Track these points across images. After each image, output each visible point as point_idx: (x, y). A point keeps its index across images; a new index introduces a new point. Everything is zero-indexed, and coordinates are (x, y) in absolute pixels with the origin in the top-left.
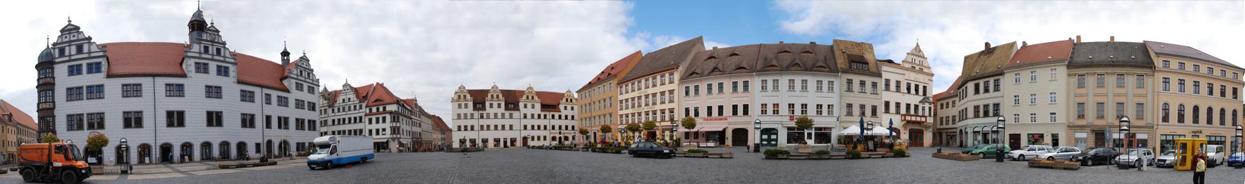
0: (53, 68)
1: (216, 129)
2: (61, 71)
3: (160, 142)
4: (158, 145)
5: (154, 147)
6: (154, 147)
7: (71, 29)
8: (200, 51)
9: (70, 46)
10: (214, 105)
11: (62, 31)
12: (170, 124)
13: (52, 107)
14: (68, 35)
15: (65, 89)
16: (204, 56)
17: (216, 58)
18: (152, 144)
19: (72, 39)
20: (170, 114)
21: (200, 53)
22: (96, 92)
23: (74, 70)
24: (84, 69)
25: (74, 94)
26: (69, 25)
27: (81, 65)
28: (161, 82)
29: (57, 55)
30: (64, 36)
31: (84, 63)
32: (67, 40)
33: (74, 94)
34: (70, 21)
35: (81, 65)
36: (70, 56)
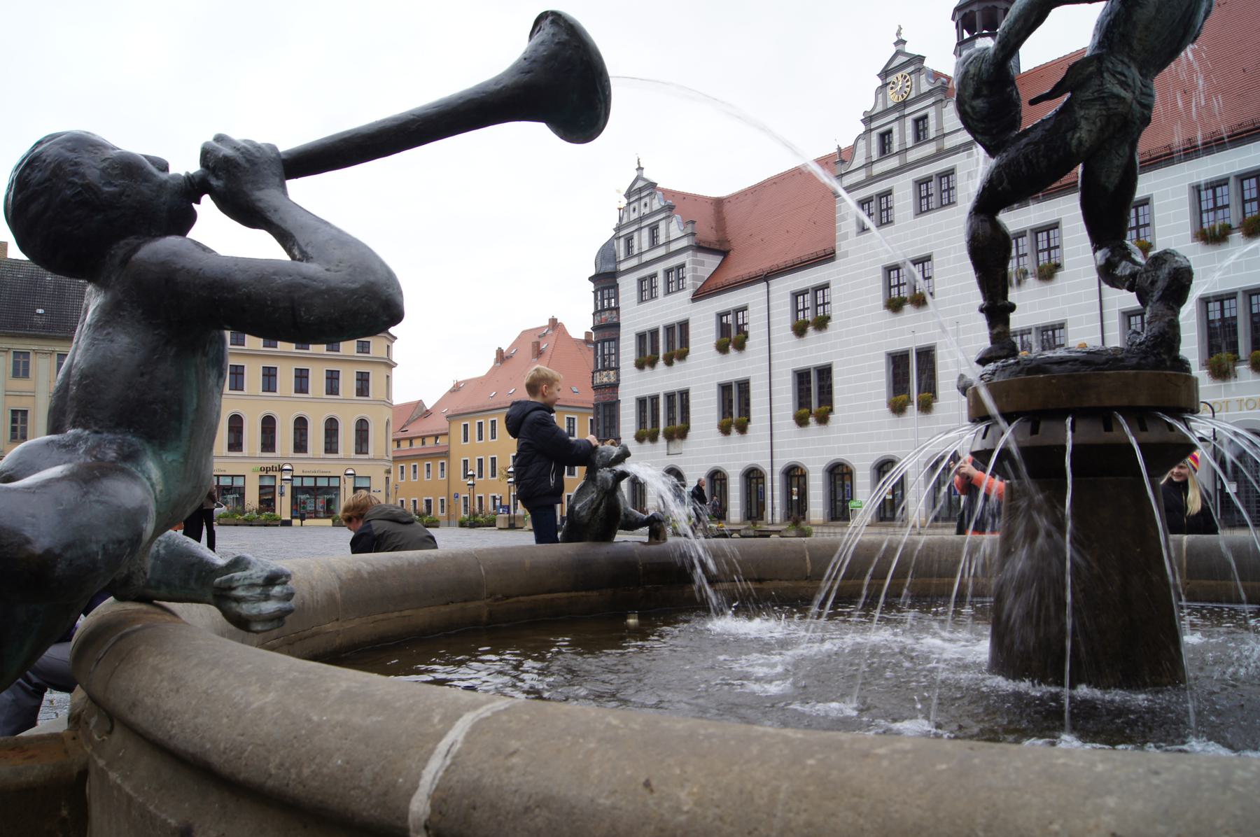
2: (628, 286)
4: (779, 468)
5: (769, 477)
6: (769, 477)
7: (640, 190)
9: (641, 228)
13: (613, 379)
15: (634, 335)
18: (766, 469)
23: (646, 290)
24: (660, 282)
29: (622, 255)
31: (659, 268)
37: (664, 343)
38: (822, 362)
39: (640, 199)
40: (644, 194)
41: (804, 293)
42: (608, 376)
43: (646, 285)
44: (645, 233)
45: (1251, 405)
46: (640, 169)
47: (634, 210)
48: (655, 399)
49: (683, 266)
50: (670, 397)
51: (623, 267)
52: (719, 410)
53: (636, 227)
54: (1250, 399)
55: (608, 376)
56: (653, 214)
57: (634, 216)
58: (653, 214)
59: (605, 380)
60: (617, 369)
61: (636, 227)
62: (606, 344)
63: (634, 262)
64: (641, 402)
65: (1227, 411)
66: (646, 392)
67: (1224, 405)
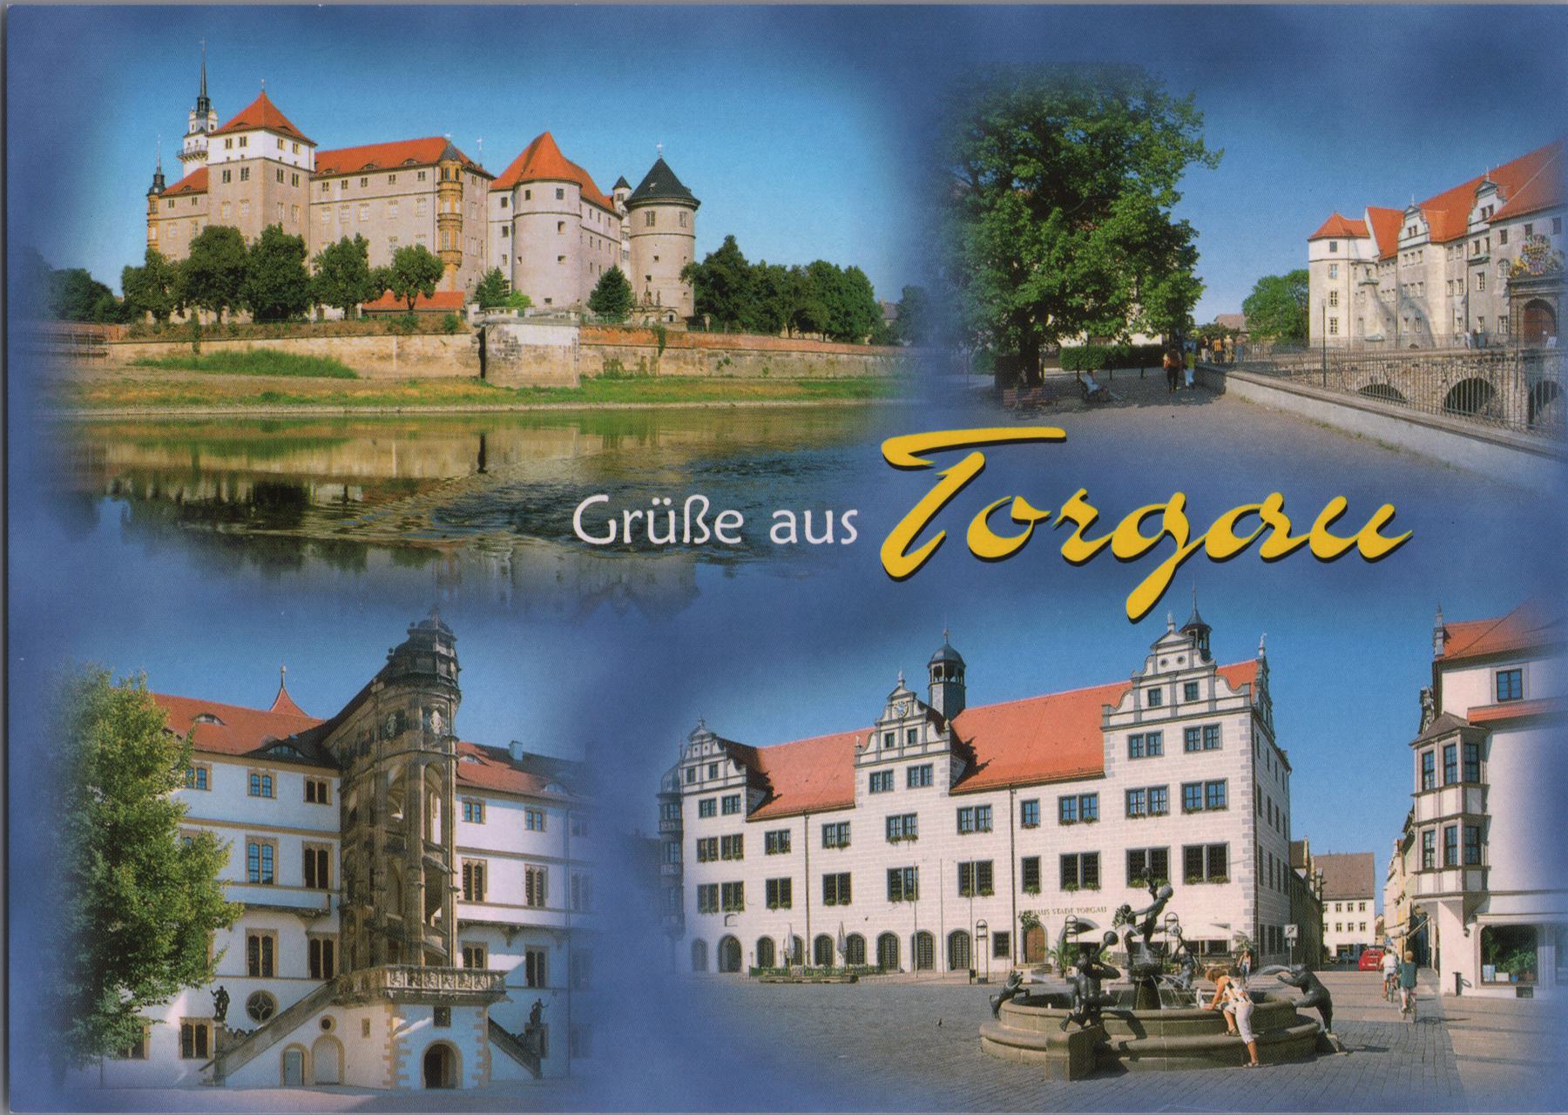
1: (904, 906)
2: (691, 806)
3: (814, 934)
4: (813, 937)
5: (806, 943)
6: (806, 943)
8: (879, 747)
9: (702, 765)
10: (902, 856)
14: (698, 746)
16: (885, 756)
18: (804, 938)
19: (706, 753)
20: (829, 880)
21: (879, 752)
22: (733, 847)
23: (707, 809)
25: (707, 850)
28: (818, 821)
31: (719, 795)
32: (696, 755)
33: (707, 850)
35: (715, 800)
39: (702, 743)
41: (832, 826)
43: (706, 805)
44: (706, 769)
49: (738, 796)
50: (726, 886)
51: (687, 790)
61: (698, 763)
62: (672, 845)
63: (697, 788)
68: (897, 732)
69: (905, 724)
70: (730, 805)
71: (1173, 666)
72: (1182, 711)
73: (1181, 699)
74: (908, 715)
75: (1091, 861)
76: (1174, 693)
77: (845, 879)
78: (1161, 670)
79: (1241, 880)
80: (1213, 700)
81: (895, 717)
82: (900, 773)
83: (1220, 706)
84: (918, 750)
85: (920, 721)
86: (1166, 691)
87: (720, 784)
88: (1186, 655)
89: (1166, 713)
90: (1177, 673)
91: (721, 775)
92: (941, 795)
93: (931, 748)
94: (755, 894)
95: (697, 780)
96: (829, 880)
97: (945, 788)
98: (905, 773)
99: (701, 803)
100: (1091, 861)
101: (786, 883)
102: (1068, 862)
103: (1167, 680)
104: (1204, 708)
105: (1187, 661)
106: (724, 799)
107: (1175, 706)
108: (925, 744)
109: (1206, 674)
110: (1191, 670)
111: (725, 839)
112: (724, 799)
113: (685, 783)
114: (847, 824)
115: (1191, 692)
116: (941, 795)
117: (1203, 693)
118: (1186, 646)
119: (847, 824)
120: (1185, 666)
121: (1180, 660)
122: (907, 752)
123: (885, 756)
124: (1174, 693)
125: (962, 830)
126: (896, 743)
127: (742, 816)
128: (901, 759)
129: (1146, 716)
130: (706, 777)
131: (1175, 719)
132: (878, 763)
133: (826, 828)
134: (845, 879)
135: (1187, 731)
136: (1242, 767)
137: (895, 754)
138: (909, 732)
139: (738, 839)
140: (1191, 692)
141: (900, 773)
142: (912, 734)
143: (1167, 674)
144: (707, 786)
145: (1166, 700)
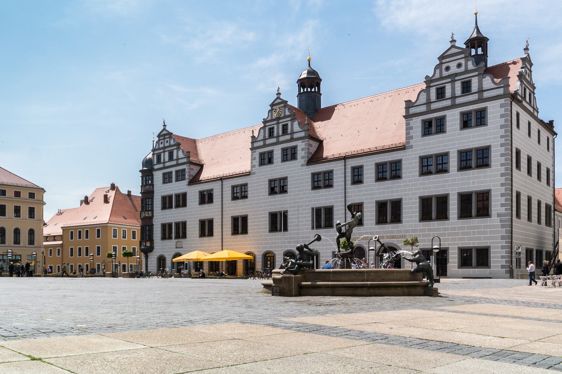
0: (152, 175)
1: (279, 236)
2: (158, 176)
7: (165, 135)
8: (265, 136)
9: (164, 152)
11: (159, 136)
12: (235, 232)
14: (163, 141)
16: (269, 141)
17: (282, 139)
19: (167, 145)
20: (235, 220)
21: (264, 140)
23: (167, 178)
25: (167, 202)
26: (164, 129)
27: (171, 172)
30: (160, 141)
31: (173, 170)
33: (167, 202)
34: (165, 126)
35: (171, 172)
36: (164, 163)
37: (175, 202)
38: (209, 217)
39: (164, 139)
40: (166, 137)
42: (148, 214)
44: (167, 154)
45: (390, 237)
46: (165, 126)
47: (162, 143)
48: (170, 225)
49: (184, 170)
52: (161, 234)
53: (162, 151)
54: (390, 236)
55: (148, 214)
56: (170, 146)
57: (161, 146)
58: (170, 146)
59: (147, 215)
60: (152, 210)
61: (162, 151)
63: (161, 166)
64: (164, 226)
65: (383, 239)
66: (167, 221)
67: (382, 237)
68: (275, 127)
69: (281, 121)
70: (180, 175)
71: (454, 69)
72: (458, 101)
73: (458, 91)
74: (282, 116)
75: (397, 205)
76: (453, 89)
77: (245, 219)
78: (445, 73)
79: (499, 215)
80: (481, 91)
81: (274, 117)
82: (277, 152)
83: (486, 95)
84: (288, 137)
85: (289, 119)
86: (448, 88)
87: (174, 163)
88: (463, 61)
89: (448, 103)
90: (456, 75)
91: (175, 157)
92: (302, 165)
93: (296, 136)
94: (193, 229)
95: (162, 161)
96: (235, 220)
97: (304, 161)
98: (280, 152)
99: (164, 174)
100: (397, 205)
101: (211, 222)
102: (381, 206)
103: (449, 80)
104: (475, 97)
105: (464, 65)
106: (177, 172)
107: (454, 97)
108: (293, 133)
109: (476, 73)
110: (467, 71)
111: (178, 196)
112: (177, 172)
113: (155, 163)
114: (246, 185)
115: (466, 88)
116: (302, 165)
117: (475, 87)
118: (463, 56)
119: (246, 185)
120: (462, 69)
121: (459, 66)
122: (282, 139)
123: (269, 141)
124: (453, 89)
125: (315, 187)
126: (275, 134)
127: (186, 182)
128: (278, 143)
129: (434, 106)
130: (167, 159)
131: (454, 106)
132: (265, 146)
133: (233, 187)
134: (245, 219)
135: (463, 114)
136: (502, 137)
137: (274, 140)
138: (283, 126)
139: (184, 195)
140: (466, 88)
141: (277, 152)
142: (285, 128)
143: (448, 77)
144: (167, 164)
145: (448, 94)
